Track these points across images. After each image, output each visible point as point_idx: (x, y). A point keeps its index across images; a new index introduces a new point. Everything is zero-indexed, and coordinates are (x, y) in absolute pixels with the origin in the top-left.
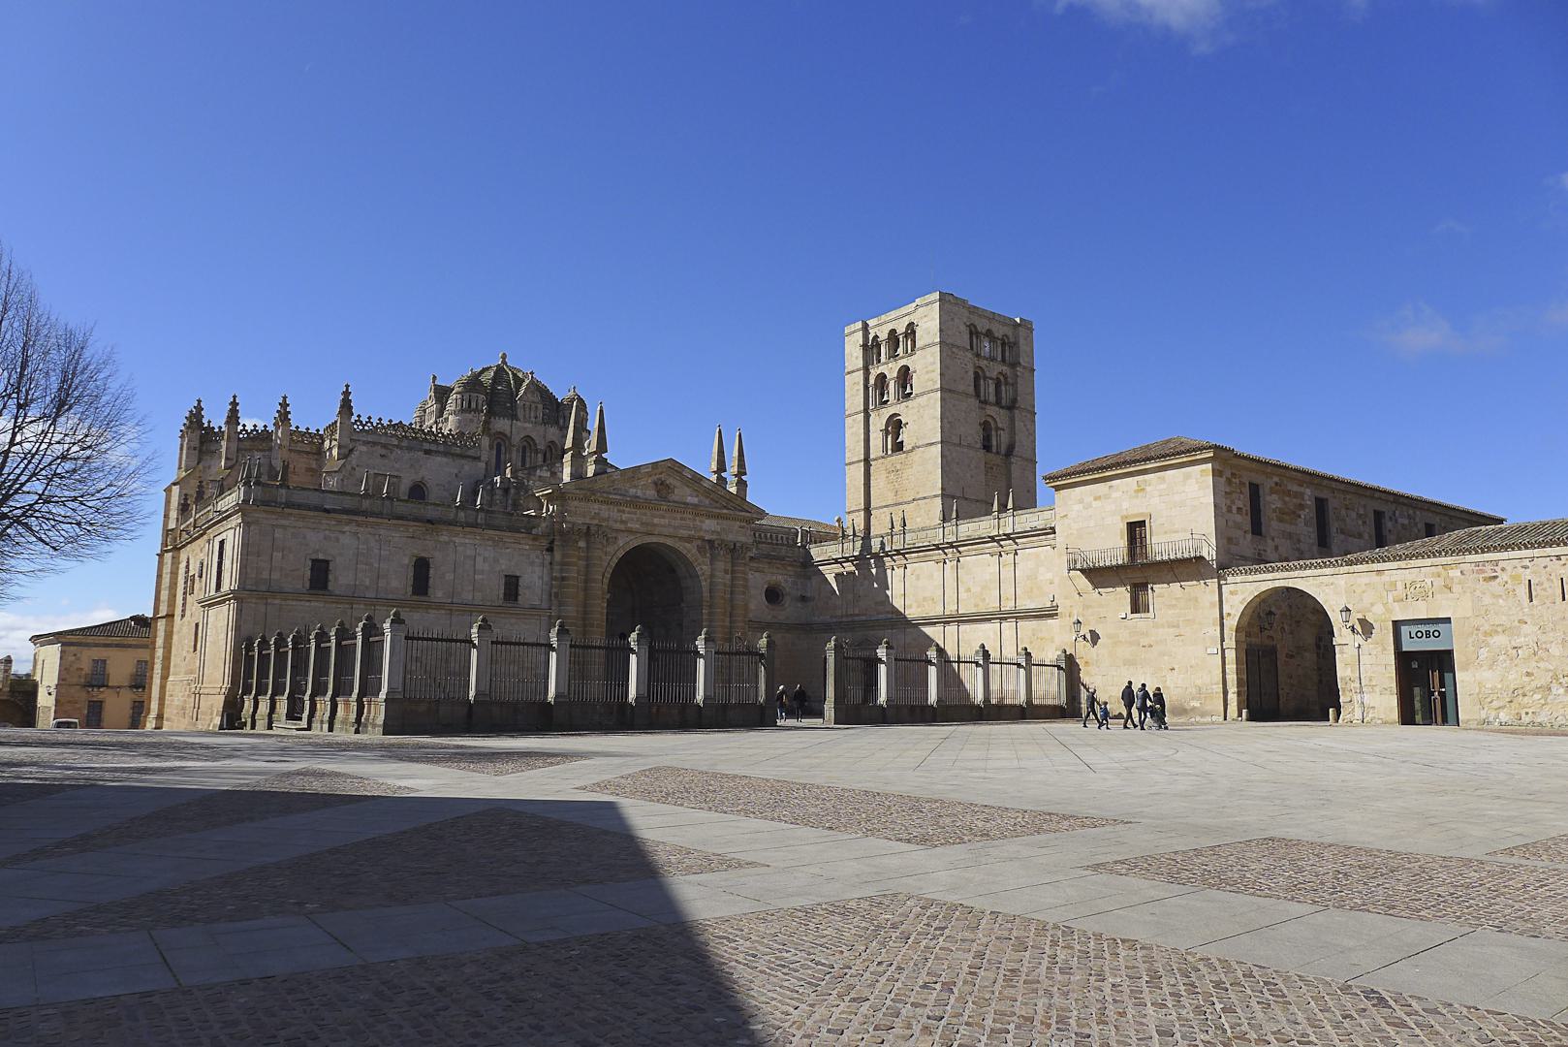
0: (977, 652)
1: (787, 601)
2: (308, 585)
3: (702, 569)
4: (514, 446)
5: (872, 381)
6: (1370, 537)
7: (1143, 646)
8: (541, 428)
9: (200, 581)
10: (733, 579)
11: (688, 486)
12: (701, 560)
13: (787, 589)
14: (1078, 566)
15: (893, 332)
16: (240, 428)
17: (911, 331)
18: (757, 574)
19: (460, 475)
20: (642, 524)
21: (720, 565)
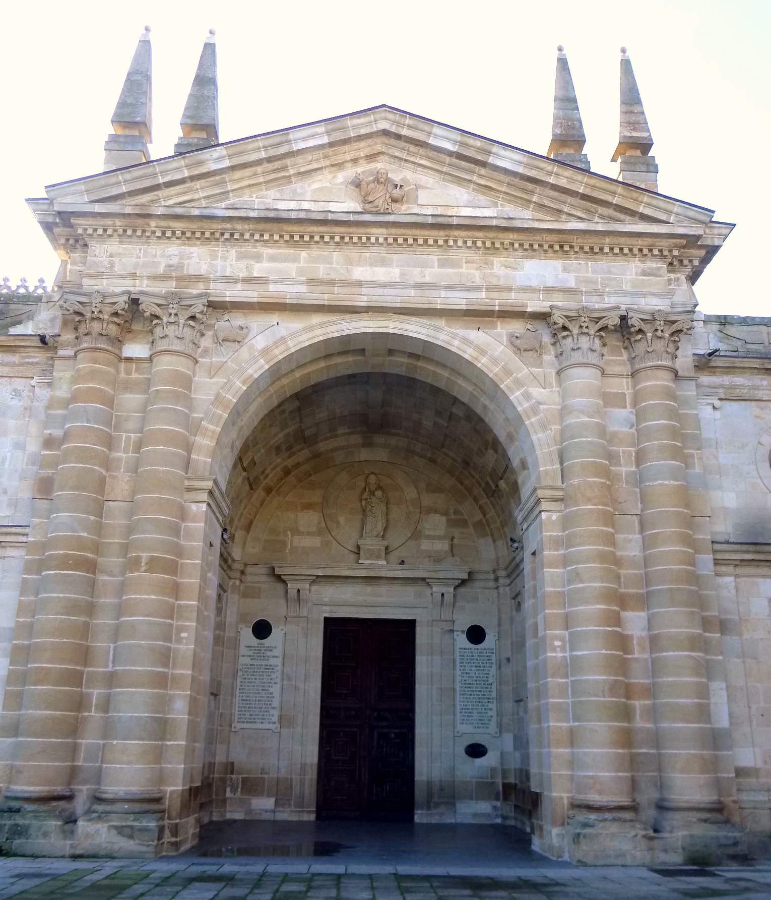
3: (527, 396)
10: (640, 416)
11: (459, 181)
12: (524, 372)
20: (313, 282)
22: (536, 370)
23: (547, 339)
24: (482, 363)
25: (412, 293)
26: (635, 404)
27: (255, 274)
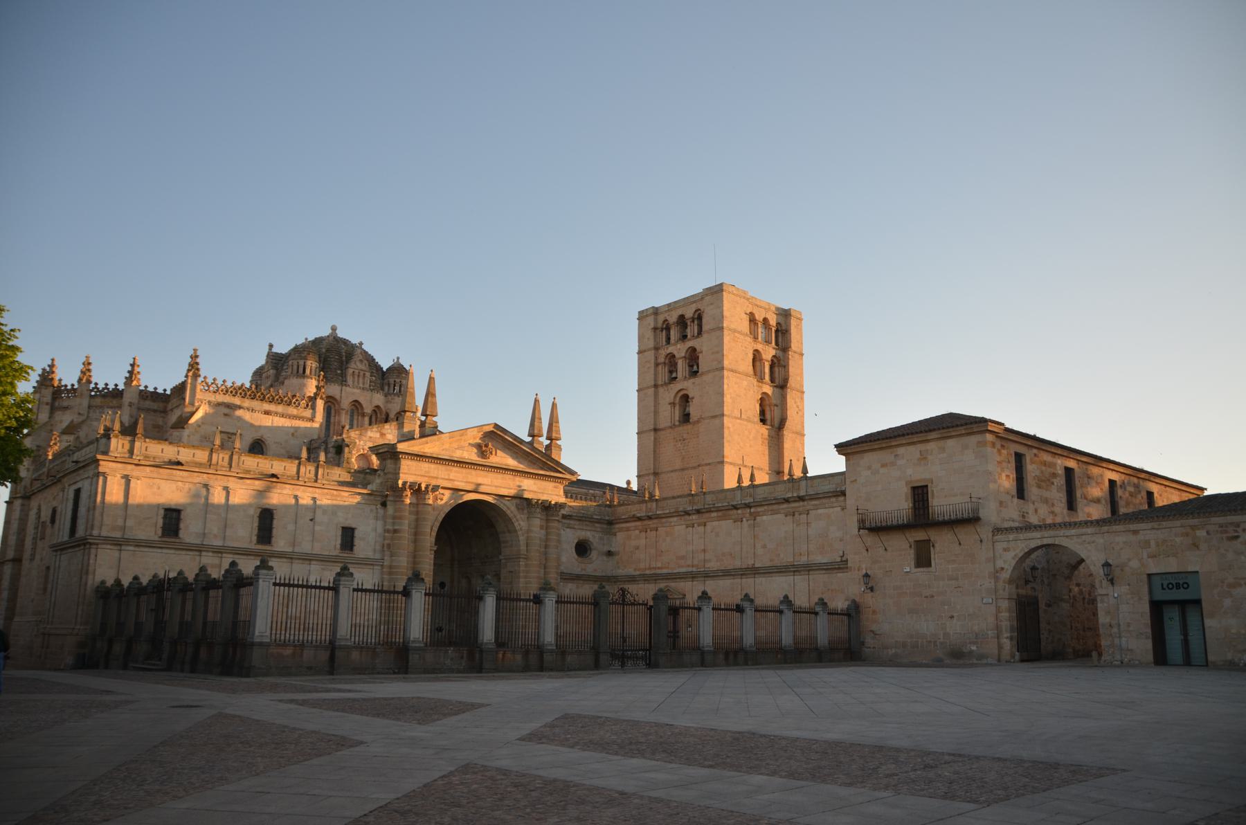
0: (781, 602)
1: (594, 554)
2: (160, 532)
3: (519, 524)
4: (343, 409)
5: (661, 360)
6: (1106, 501)
7: (926, 597)
8: (368, 394)
9: (52, 527)
10: (547, 534)
11: (508, 449)
13: (595, 544)
14: (867, 525)
15: (682, 317)
16: (92, 386)
17: (699, 317)
18: (568, 530)
19: (295, 434)
20: (466, 482)
21: (537, 522)
22: (522, 516)
23: (525, 504)
24: (508, 512)
25: (494, 488)
26: (546, 529)
27: (451, 478)
